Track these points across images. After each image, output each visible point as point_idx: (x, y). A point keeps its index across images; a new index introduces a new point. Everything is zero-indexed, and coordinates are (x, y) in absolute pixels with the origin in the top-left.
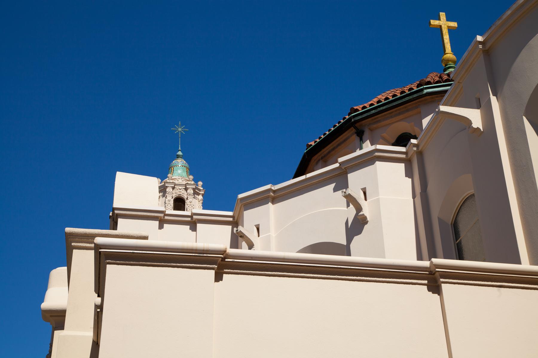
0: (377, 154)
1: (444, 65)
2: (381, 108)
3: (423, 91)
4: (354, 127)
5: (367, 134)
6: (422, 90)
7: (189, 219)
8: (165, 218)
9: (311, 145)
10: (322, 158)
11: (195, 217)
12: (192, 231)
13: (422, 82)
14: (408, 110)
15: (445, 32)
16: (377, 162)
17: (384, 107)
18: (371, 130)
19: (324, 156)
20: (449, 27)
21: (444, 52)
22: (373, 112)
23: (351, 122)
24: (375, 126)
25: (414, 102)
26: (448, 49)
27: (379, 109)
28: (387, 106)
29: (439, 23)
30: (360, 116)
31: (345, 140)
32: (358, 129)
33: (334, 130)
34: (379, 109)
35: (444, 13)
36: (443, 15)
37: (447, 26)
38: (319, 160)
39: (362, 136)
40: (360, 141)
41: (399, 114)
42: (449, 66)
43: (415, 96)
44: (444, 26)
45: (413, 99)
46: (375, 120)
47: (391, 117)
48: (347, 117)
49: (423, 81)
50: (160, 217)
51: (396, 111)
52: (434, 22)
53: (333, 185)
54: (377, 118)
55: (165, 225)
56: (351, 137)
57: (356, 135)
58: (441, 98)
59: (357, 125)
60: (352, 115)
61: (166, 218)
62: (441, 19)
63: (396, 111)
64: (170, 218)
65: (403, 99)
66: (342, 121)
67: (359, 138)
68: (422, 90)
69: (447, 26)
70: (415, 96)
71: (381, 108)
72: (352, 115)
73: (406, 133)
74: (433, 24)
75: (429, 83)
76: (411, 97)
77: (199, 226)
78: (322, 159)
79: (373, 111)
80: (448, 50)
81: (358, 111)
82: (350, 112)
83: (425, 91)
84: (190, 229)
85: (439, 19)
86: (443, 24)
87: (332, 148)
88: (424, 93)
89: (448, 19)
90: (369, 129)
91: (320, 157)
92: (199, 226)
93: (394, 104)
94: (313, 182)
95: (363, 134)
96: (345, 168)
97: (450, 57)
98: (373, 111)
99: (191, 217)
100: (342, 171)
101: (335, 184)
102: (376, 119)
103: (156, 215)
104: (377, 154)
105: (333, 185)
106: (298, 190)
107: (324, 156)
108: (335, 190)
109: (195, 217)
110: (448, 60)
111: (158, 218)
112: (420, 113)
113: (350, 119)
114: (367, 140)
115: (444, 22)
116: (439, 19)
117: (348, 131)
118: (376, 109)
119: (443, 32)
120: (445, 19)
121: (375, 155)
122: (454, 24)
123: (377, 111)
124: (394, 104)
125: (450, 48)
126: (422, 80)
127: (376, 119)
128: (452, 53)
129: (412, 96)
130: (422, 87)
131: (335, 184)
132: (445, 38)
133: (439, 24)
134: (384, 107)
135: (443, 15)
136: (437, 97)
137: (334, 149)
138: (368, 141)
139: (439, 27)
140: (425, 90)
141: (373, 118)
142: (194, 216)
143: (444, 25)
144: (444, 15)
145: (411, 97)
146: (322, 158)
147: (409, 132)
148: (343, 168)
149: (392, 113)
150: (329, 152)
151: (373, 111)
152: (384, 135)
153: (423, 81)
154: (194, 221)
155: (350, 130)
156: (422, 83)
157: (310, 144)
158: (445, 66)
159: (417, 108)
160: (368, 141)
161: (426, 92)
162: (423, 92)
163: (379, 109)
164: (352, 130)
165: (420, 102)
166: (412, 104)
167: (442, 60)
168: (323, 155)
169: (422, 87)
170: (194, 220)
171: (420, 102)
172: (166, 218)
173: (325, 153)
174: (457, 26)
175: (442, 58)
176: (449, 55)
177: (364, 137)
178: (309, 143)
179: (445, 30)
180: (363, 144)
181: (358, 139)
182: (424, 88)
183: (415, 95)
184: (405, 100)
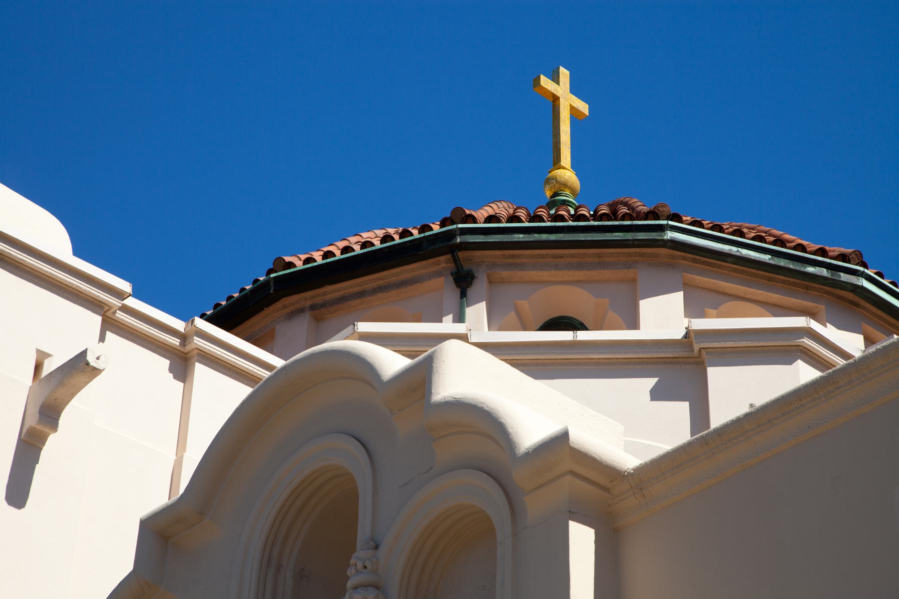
0: (807, 342)
1: (548, 194)
2: (544, 237)
3: (663, 231)
4: (453, 256)
5: (480, 285)
6: (661, 229)
7: (175, 342)
8: (117, 314)
9: (291, 265)
10: (313, 308)
11: (198, 342)
12: (175, 377)
13: (661, 209)
14: (603, 265)
15: (565, 116)
16: (799, 360)
17: (553, 237)
18: (491, 282)
19: (324, 305)
20: (573, 109)
21: (556, 162)
22: (519, 238)
23: (451, 243)
24: (505, 273)
25: (626, 250)
26: (566, 159)
27: (537, 237)
28: (561, 235)
29: (556, 90)
30: (482, 236)
31: (404, 284)
32: (462, 269)
33: (381, 249)
34: (537, 237)
35: (567, 72)
36: (564, 73)
37: (570, 105)
38: (302, 311)
39: (468, 287)
40: (461, 298)
41: (580, 266)
42: (565, 198)
43: (641, 236)
44: (563, 100)
45: (631, 242)
46: (510, 261)
47: (556, 267)
48: (436, 229)
49: (664, 209)
50: (107, 308)
51: (572, 256)
52: (546, 82)
53: (651, 382)
54: (519, 256)
55: (109, 335)
56: (430, 279)
57: (451, 279)
58: (692, 264)
59: (461, 255)
60: (460, 226)
61: (120, 315)
62: (561, 83)
63: (572, 256)
64: (129, 321)
65: (607, 234)
66: (415, 232)
67: (459, 290)
68: (661, 229)
69: (570, 105)
70: (641, 236)
71: (544, 237)
72: (460, 226)
73: (574, 318)
74: (544, 86)
75: (677, 217)
76: (629, 236)
77: (200, 370)
78: (313, 310)
79: (521, 236)
80: (565, 161)
81: (475, 221)
82: (448, 215)
83: (670, 235)
84: (171, 370)
85: (556, 79)
86: (562, 94)
87: (358, 289)
88: (665, 237)
89: (574, 90)
90: (488, 276)
91: (308, 303)
92: (200, 370)
93: (582, 237)
94: (592, 356)
95: (471, 285)
96: (700, 349)
97: (570, 177)
98: (521, 237)
99: (184, 338)
100: (685, 354)
101: (656, 379)
102: (513, 256)
103: (101, 296)
104: (807, 342)
105: (651, 382)
106: (537, 365)
107: (324, 305)
108: (657, 394)
109: (198, 342)
110: (565, 185)
111: (103, 308)
112: (634, 280)
113: (449, 236)
114: (483, 301)
115: (565, 92)
116: (556, 79)
117: (425, 262)
118: (530, 234)
119: (561, 115)
120: (568, 86)
121: (803, 342)
122: (583, 107)
123: (532, 240)
124: (582, 237)
125: (569, 159)
126: (662, 206)
127: (513, 256)
128: (572, 170)
129: (633, 234)
130: (664, 222)
131: (656, 379)
132: (563, 130)
133: (555, 93)
134: (553, 237)
135: (564, 73)
136: (684, 258)
137: (361, 294)
138: (484, 303)
139: (551, 99)
140: (668, 231)
141: (507, 252)
142: (195, 338)
143: (565, 99)
144: (566, 76)
145: (629, 236)
146: (313, 308)
147: (581, 320)
148: (696, 347)
149: (561, 257)
150: (343, 299)
151: (521, 237)
152: (524, 304)
153: (664, 209)
154: (186, 352)
155: (430, 261)
156: (660, 212)
157: (288, 259)
158: (552, 197)
159: (629, 268)
160: (485, 302)
161: (672, 237)
162: (663, 234)
163: (536, 235)
164: (443, 262)
165: (640, 256)
166: (618, 253)
167: (548, 179)
168: (319, 300)
169: (664, 222)
170: (189, 348)
171: (641, 255)
172: (120, 315)
173: (328, 297)
174: (588, 114)
175: (551, 174)
176: (567, 174)
177: (471, 292)
178: (285, 258)
179: (565, 112)
180: (467, 307)
181: (451, 293)
182: (667, 224)
183: (642, 234)
184: (611, 237)
